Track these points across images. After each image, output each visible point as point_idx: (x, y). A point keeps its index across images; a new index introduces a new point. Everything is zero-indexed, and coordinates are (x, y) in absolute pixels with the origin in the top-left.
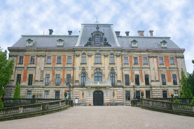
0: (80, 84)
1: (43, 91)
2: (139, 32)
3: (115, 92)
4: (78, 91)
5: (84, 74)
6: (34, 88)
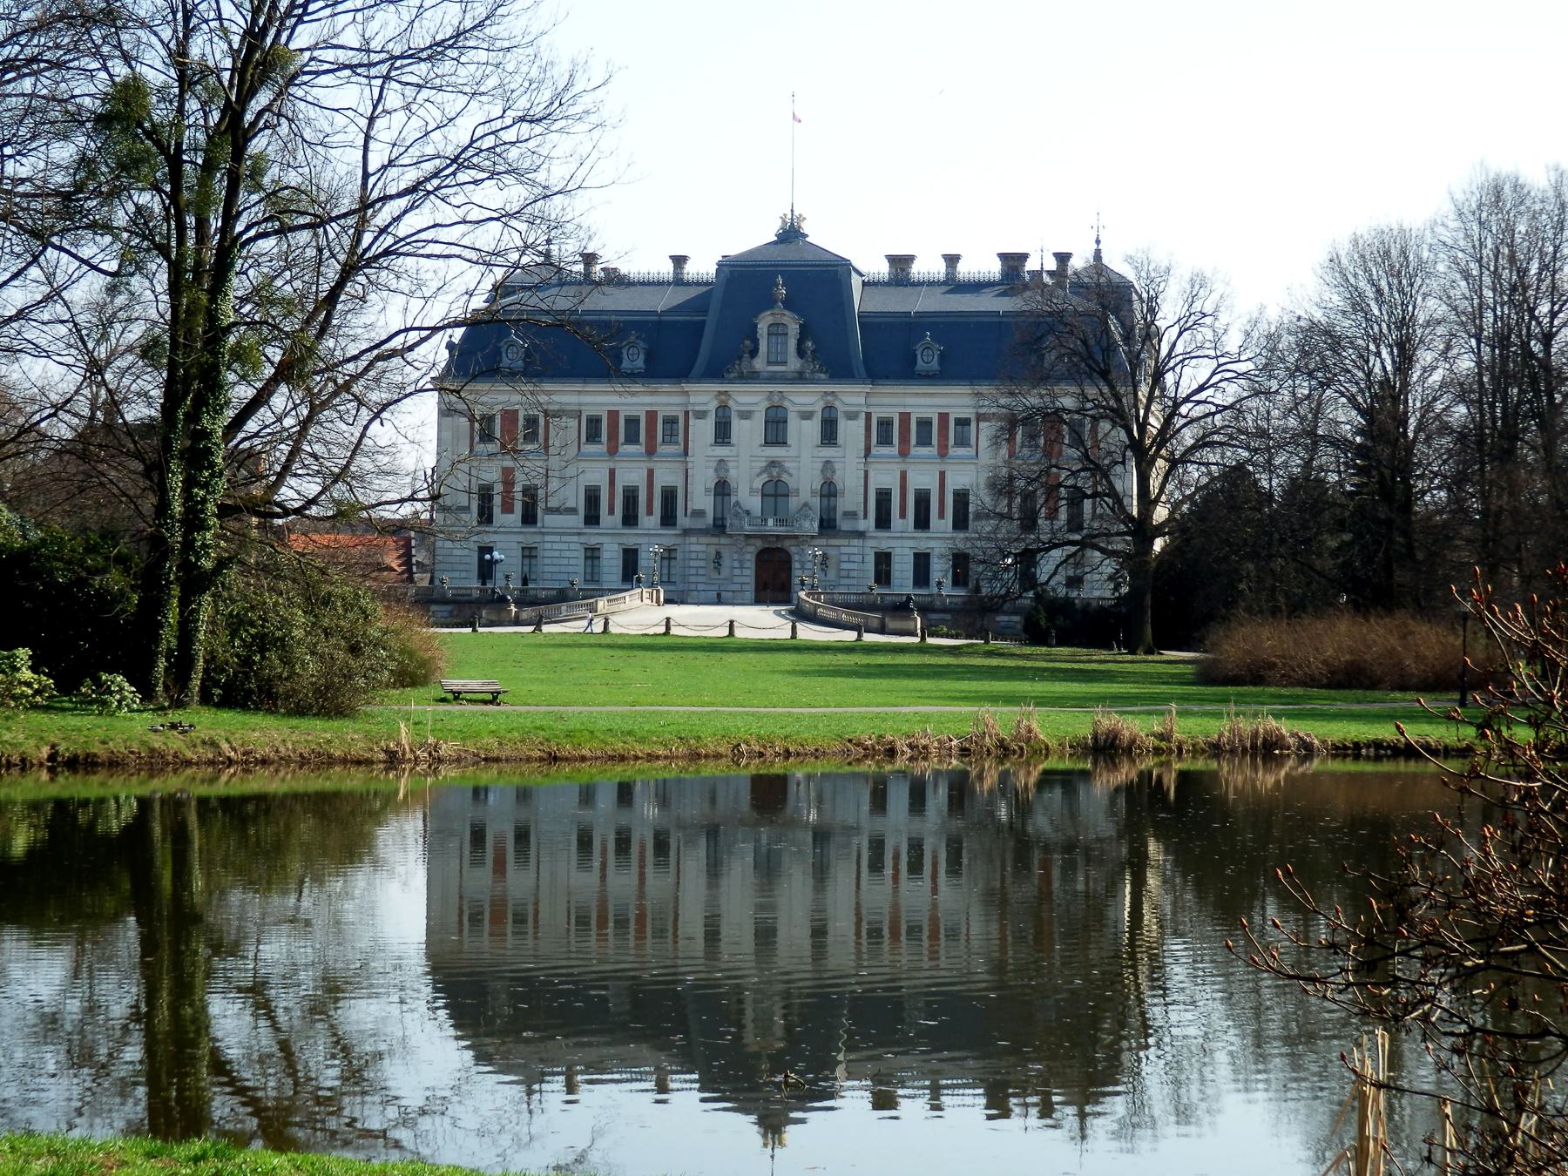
0: (710, 519)
1: (578, 546)
2: (1004, 257)
3: (832, 552)
4: (703, 548)
5: (722, 489)
6: (547, 538)
